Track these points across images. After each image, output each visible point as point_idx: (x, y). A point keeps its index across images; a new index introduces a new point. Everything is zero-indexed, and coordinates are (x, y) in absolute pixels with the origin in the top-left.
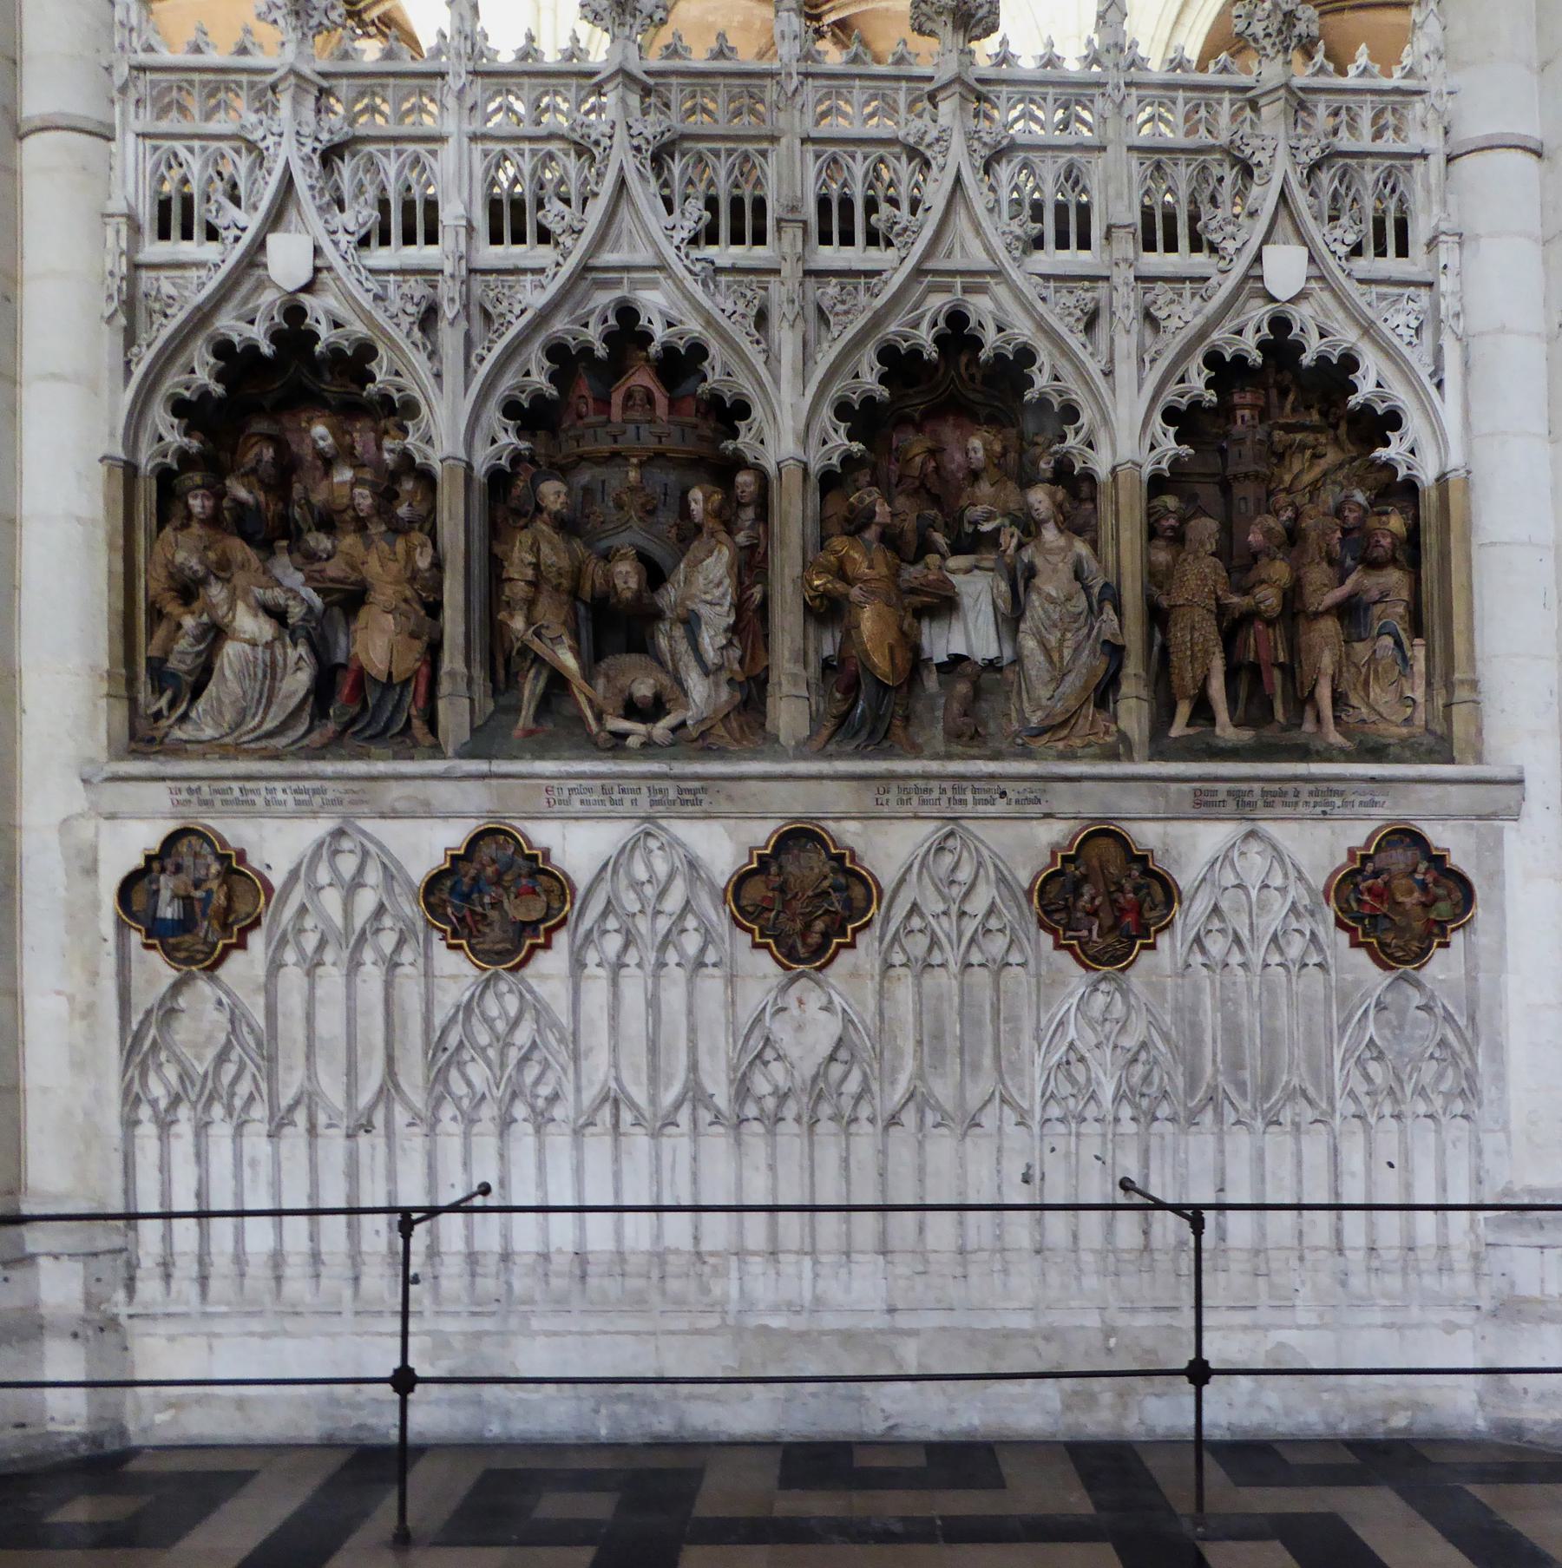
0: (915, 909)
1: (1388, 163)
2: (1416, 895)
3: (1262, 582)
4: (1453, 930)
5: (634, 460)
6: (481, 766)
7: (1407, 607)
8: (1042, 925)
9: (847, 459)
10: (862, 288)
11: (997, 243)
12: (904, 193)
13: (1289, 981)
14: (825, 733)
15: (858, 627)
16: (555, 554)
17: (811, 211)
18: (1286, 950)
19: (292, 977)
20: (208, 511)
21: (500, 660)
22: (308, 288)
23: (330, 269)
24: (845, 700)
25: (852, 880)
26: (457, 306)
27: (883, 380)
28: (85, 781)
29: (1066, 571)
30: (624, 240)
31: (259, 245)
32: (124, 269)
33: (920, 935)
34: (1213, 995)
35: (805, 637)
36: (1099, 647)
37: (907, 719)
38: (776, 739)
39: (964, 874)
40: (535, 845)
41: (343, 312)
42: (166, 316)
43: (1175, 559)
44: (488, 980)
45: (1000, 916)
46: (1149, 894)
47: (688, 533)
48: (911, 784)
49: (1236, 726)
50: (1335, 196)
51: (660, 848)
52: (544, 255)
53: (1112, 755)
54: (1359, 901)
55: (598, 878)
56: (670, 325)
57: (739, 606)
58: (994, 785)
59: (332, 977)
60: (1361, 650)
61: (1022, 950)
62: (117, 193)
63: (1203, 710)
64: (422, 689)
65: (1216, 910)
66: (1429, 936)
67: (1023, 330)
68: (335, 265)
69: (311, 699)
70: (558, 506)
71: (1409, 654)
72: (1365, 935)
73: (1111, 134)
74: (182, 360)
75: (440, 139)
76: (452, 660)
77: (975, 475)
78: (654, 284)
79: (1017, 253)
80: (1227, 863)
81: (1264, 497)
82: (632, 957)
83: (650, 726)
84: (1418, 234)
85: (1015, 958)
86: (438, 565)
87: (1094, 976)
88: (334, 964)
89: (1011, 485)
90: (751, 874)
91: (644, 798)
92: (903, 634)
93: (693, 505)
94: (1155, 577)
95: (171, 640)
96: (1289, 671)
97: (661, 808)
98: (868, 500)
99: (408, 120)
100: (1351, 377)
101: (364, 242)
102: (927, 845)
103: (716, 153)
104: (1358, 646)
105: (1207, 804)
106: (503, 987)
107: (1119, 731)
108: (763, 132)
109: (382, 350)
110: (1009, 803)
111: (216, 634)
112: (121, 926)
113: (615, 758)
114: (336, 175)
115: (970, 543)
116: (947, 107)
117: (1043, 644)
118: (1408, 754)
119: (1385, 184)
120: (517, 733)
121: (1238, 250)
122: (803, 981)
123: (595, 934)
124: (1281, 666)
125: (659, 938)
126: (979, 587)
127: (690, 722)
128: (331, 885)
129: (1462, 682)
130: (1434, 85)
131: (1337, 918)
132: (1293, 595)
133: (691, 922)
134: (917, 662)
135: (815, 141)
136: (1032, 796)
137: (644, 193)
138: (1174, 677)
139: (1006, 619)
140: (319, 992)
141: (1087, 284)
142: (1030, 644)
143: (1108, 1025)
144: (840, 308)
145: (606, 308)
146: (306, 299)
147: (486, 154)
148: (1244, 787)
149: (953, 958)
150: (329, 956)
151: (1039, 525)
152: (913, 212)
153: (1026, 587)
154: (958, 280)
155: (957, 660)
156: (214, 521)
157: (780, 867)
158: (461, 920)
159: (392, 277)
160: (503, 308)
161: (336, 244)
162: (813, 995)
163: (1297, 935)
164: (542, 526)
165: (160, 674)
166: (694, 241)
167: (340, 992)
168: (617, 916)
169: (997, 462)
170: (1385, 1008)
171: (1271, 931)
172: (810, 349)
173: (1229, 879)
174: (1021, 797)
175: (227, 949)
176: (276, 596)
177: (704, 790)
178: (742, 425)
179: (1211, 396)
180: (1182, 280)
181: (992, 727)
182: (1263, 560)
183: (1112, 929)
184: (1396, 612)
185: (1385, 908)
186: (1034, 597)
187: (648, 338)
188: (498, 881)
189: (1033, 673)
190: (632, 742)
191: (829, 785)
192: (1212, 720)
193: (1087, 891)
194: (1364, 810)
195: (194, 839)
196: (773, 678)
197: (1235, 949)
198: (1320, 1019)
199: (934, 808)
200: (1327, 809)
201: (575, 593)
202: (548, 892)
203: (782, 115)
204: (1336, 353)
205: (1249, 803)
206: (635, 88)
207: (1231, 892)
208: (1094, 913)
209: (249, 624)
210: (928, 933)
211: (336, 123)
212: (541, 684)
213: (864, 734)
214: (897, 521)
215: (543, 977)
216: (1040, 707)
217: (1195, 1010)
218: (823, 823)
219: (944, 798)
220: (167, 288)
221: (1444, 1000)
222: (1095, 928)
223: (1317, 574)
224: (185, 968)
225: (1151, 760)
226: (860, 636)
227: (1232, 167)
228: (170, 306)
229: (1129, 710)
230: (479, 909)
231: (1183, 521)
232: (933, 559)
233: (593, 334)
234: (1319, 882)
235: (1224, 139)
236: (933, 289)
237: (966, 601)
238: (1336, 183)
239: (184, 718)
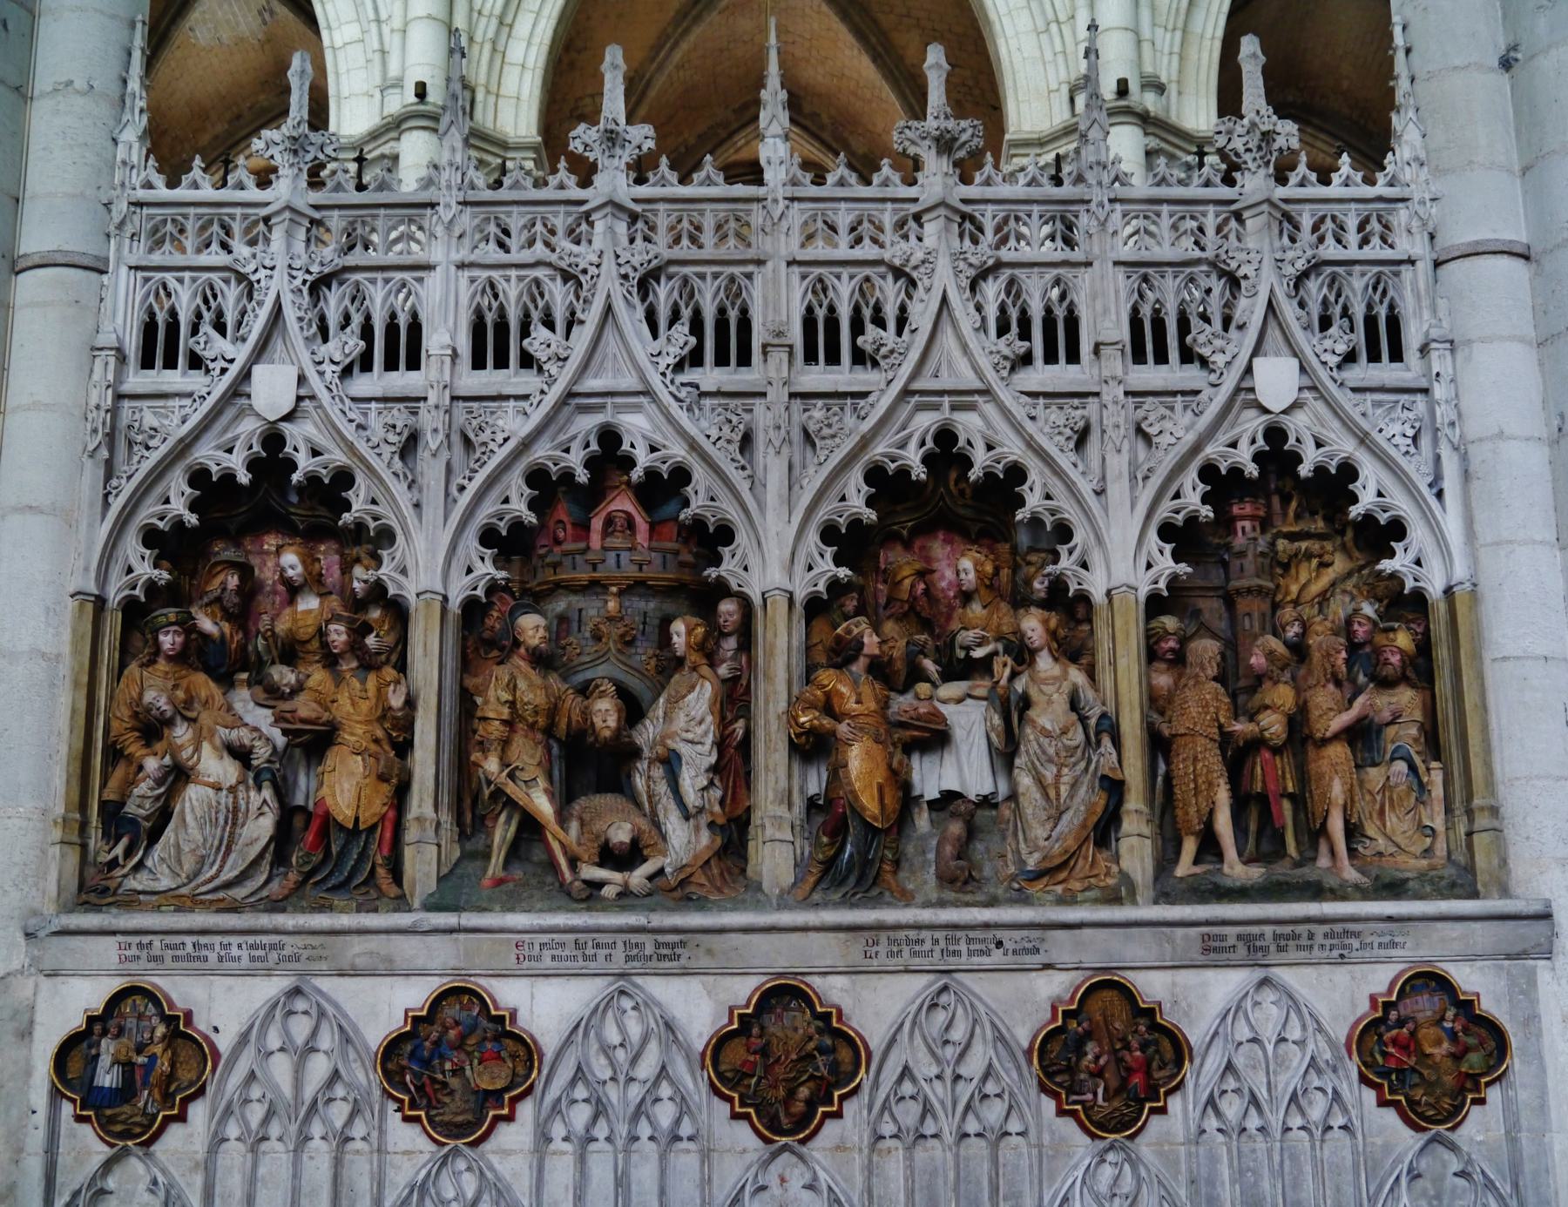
0: (906, 1072)
1: (1376, 269)
2: (1446, 1045)
3: (1267, 707)
4: (1488, 1084)
5: (614, 589)
6: (448, 919)
7: (1422, 727)
8: (1043, 1088)
9: (834, 585)
10: (848, 409)
11: (985, 363)
12: (890, 312)
13: (1313, 1147)
14: (812, 879)
15: (846, 766)
16: (532, 690)
17: (796, 335)
18: (1308, 1111)
19: (234, 1154)
20: (177, 647)
21: (468, 802)
22: (289, 417)
23: (312, 397)
24: (831, 844)
25: (840, 1043)
26: (441, 436)
27: (870, 502)
28: (29, 935)
29: (1060, 702)
30: (609, 364)
31: (245, 375)
32: (109, 402)
33: (912, 1102)
34: (1231, 1165)
35: (790, 776)
37: (897, 864)
38: (759, 888)
39: (958, 1034)
40: (502, 1004)
41: (322, 440)
42: (148, 448)
43: (1176, 684)
44: (446, 1157)
45: (998, 1079)
46: (1157, 1051)
47: (670, 665)
48: (902, 934)
49: (1245, 863)
50: (1325, 302)
51: (634, 1008)
52: (526, 381)
53: (1113, 899)
54: (1385, 1054)
55: (568, 1041)
56: (653, 449)
57: (721, 744)
58: (989, 934)
59: (276, 1156)
60: (1375, 775)
61: (1022, 1117)
62: (107, 326)
63: (1209, 846)
64: (388, 835)
65: (1230, 1067)
66: (1462, 1091)
67: (1013, 449)
68: (320, 395)
69: (272, 847)
70: (536, 642)
71: (1425, 779)
72: (1392, 1092)
73: (1096, 250)
74: (158, 490)
75: (429, 267)
76: (421, 803)
77: (966, 597)
78: (638, 408)
79: (1005, 373)
80: (1241, 1014)
81: (1269, 613)
82: (601, 1130)
83: (626, 874)
84: (1412, 337)
85: (1014, 1126)
86: (410, 703)
87: (1101, 1145)
88: (280, 1139)
89: (1004, 607)
90: (731, 1035)
91: (619, 954)
93: (675, 638)
94: (1155, 702)
95: (130, 783)
96: (1298, 801)
97: (635, 964)
99: (398, 247)
100: (1351, 487)
101: (347, 372)
102: (919, 1001)
103: (702, 277)
104: (1373, 772)
105: (1215, 950)
106: (461, 1164)
107: (1121, 871)
108: (749, 257)
109: (360, 479)
110: (1005, 954)
111: (179, 775)
112: (56, 1095)
113: (589, 909)
114: (322, 303)
115: (960, 668)
116: (931, 228)
117: (1039, 781)
118: (1428, 889)
119: (1375, 289)
120: (486, 882)
121: (1228, 363)
122: (786, 1155)
123: (564, 1103)
124: (1291, 797)
125: (632, 1109)
126: (973, 717)
127: (668, 870)
128: (282, 1049)
129: (1482, 809)
130: (1416, 193)
131: (1361, 1073)
132: (1298, 722)
133: (665, 1090)
134: (908, 800)
135: (800, 263)
136: (1029, 946)
137: (631, 319)
138: (1179, 812)
139: (1000, 753)
140: (262, 1171)
141: (1076, 402)
142: (1025, 781)
143: (1117, 1201)
144: (826, 431)
145: (588, 433)
146: (286, 428)
147: (473, 280)
148: (1255, 930)
149: (948, 1128)
150: (275, 1129)
151: (1033, 652)
152: (899, 333)
153: (1021, 719)
154: (946, 399)
155: (949, 797)
156: (180, 658)
157: (762, 1028)
158: (420, 1089)
159: (373, 405)
160: (485, 437)
161: (322, 374)
162: (797, 1172)
163: (1319, 1094)
164: (519, 663)
165: (114, 819)
166: (679, 367)
167: (285, 1173)
168: (587, 1084)
169: (989, 584)
170: (1419, 1176)
171: (1290, 1090)
172: (796, 471)
173: (1244, 1032)
174: (1018, 947)
175: (168, 1120)
176: (242, 736)
177: (683, 944)
178: (726, 551)
179: (1207, 512)
180: (1174, 394)
181: (987, 871)
182: (1267, 685)
183: (1118, 1092)
184: (1407, 734)
185: (1412, 1061)
186: (1028, 730)
187: (630, 462)
188: (460, 1045)
189: (1029, 811)
190: (609, 892)
191: (812, 935)
192: (1220, 856)
193: (1091, 1048)
194: (1383, 952)
195: (138, 999)
196: (756, 818)
197: (1253, 1111)
198: (1349, 1190)
199: (926, 961)
200: (1345, 952)
201: (549, 731)
202: (514, 1057)
203: (768, 238)
204: (1334, 463)
205: (1261, 948)
206: (621, 215)
207: (1246, 1047)
208: (1098, 1074)
209: (216, 767)
210: (920, 1099)
211: (328, 255)
212: (513, 828)
213: (852, 880)
214: (885, 648)
215: (505, 1153)
216: (1037, 848)
217: (1212, 1182)
218: (808, 979)
219: (937, 949)
220: (150, 420)
221: (1482, 1163)
222: (1100, 1091)
223: (1323, 697)
224: (121, 1144)
225: (1156, 902)
226: (848, 776)
227: (1220, 278)
228: (152, 437)
229: (1132, 848)
230: (440, 1077)
231: (1184, 640)
232: (923, 688)
233: (575, 460)
234: (1340, 1033)
235: (1209, 254)
236: (920, 408)
237: (958, 734)
238: (1325, 290)
239: (140, 866)
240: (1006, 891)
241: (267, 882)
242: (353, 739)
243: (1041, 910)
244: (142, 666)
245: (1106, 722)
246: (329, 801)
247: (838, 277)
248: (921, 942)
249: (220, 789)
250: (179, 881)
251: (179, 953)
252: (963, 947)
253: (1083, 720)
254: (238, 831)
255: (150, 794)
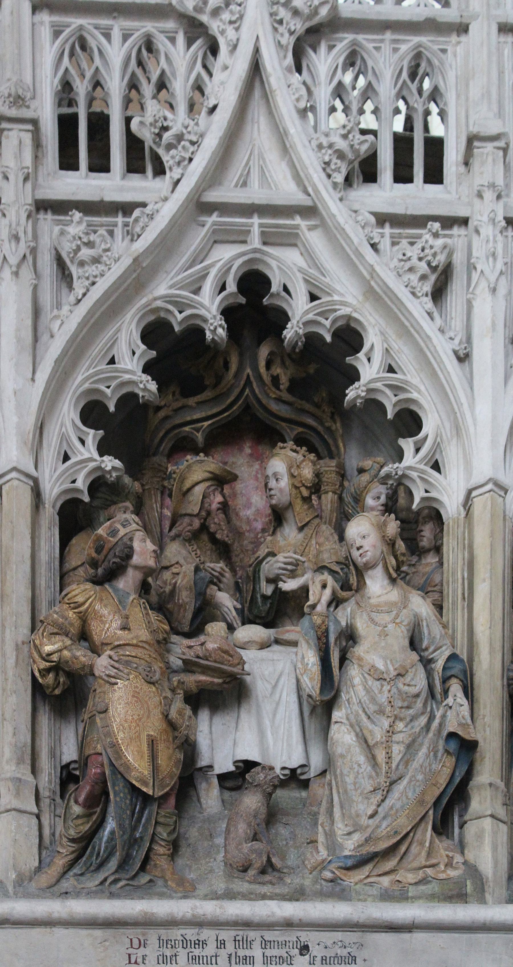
36: (441, 743)
48: (176, 934)
58: (291, 936)
92: (172, 725)
98: (122, 532)
136: (344, 952)
153: (343, 659)
174: (329, 953)
181: (292, 859)
189: (349, 780)
191: (60, 932)
213: (113, 864)
219: (223, 954)
240: (315, 882)
243: (360, 905)
245: (456, 669)
247: (108, 36)
248: (201, 944)
252: (257, 952)
253: (427, 663)
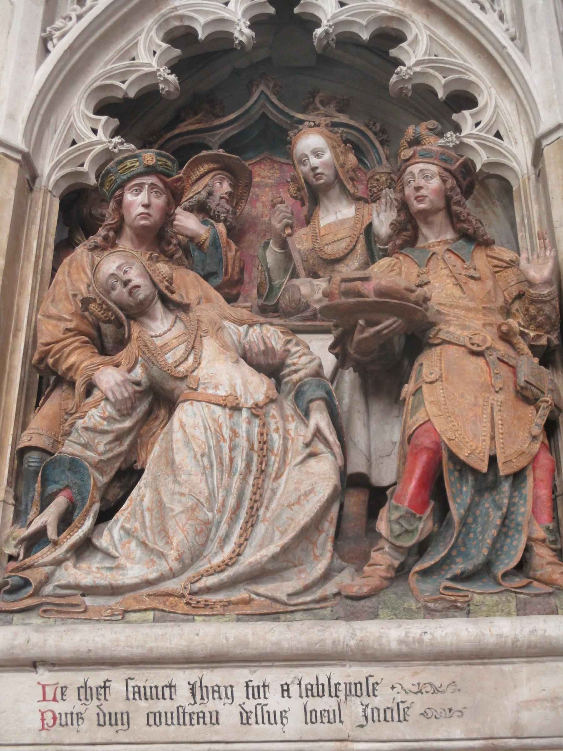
241: (326, 577)
242: (466, 333)
244: (95, 248)
246: (439, 424)
249: (236, 409)
250: (163, 567)
251: (163, 706)
254: (269, 484)
255: (105, 426)
